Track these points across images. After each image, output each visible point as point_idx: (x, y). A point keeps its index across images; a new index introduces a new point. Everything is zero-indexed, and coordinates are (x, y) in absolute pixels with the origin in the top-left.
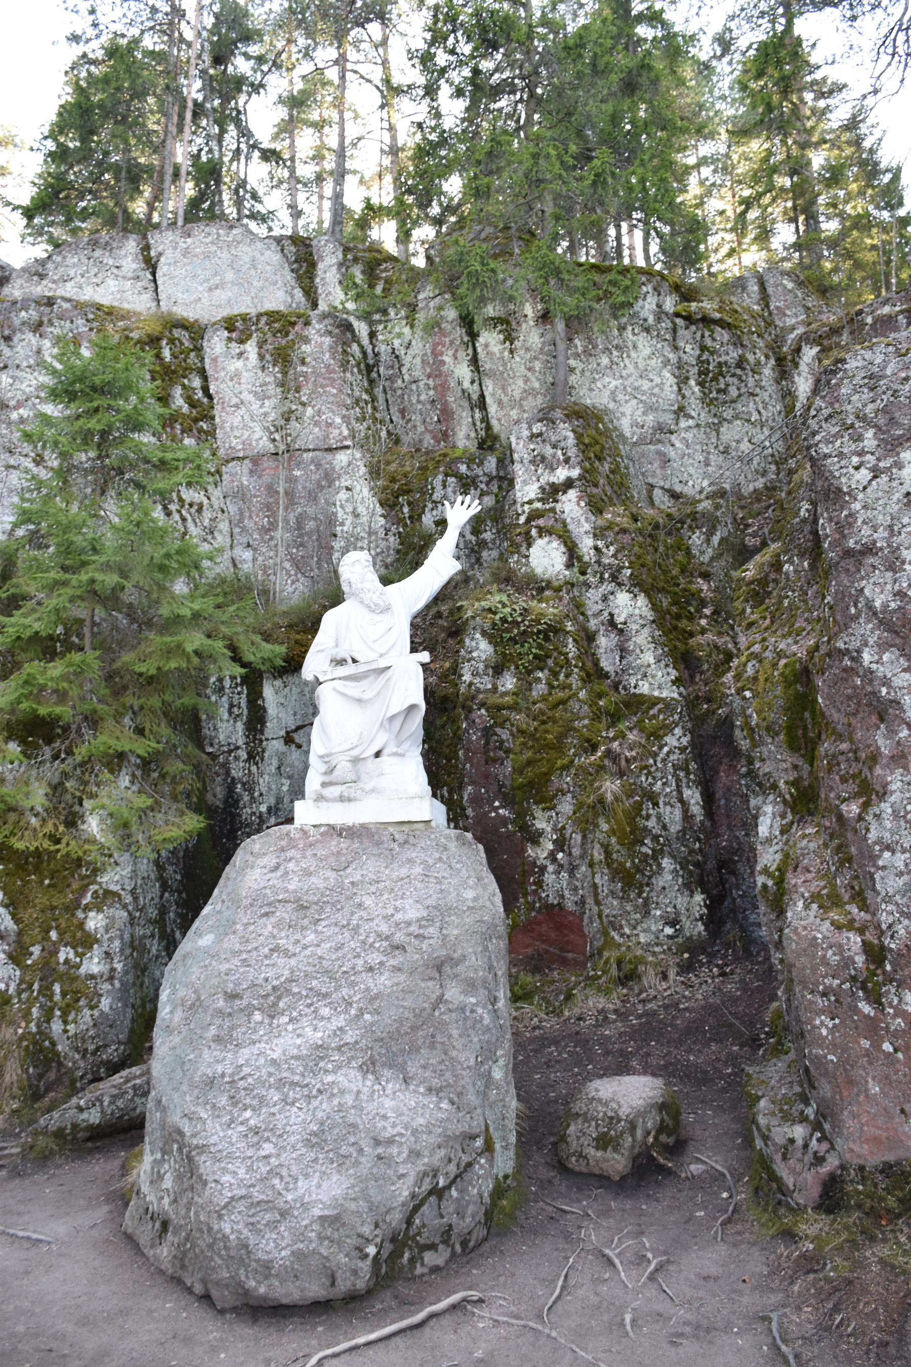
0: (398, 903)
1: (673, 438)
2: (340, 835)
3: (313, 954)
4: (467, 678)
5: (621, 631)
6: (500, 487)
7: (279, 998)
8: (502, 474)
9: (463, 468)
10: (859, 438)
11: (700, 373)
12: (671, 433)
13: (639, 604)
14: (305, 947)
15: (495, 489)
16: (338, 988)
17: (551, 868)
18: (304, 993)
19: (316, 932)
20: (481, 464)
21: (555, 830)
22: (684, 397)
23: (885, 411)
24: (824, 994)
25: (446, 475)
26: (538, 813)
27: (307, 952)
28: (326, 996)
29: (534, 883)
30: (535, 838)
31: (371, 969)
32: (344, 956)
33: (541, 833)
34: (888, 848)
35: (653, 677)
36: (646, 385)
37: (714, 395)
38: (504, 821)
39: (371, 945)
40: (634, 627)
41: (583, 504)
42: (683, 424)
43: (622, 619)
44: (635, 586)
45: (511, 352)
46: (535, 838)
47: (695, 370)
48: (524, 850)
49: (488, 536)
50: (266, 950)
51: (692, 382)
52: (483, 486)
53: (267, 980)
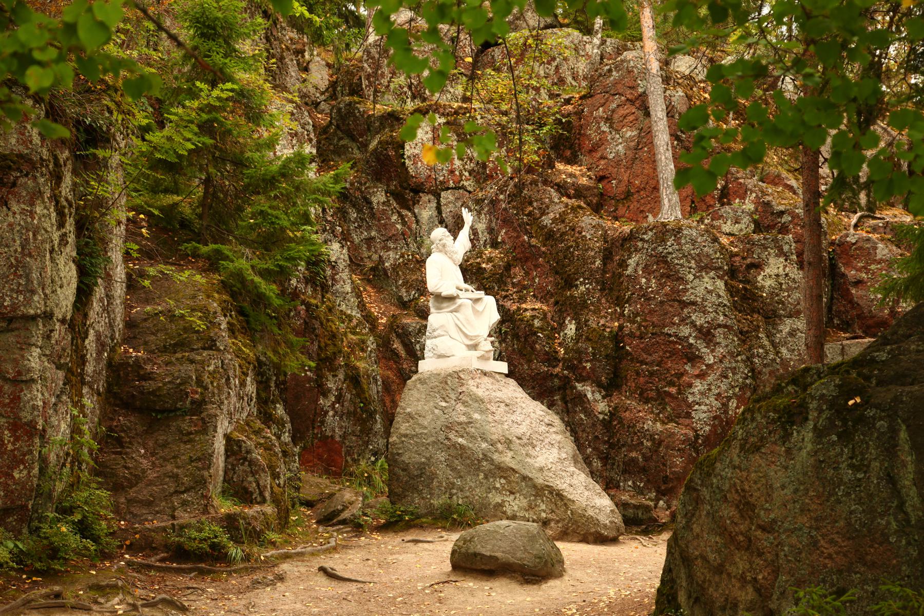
4: (294, 282)
5: (334, 267)
10: (689, 262)
13: (344, 251)
17: (331, 413)
21: (337, 389)
23: (698, 255)
24: (679, 450)
26: (330, 378)
29: (320, 422)
30: (325, 393)
33: (329, 390)
34: (697, 404)
38: (309, 379)
40: (342, 267)
43: (333, 259)
44: (343, 239)
46: (325, 393)
48: (318, 400)
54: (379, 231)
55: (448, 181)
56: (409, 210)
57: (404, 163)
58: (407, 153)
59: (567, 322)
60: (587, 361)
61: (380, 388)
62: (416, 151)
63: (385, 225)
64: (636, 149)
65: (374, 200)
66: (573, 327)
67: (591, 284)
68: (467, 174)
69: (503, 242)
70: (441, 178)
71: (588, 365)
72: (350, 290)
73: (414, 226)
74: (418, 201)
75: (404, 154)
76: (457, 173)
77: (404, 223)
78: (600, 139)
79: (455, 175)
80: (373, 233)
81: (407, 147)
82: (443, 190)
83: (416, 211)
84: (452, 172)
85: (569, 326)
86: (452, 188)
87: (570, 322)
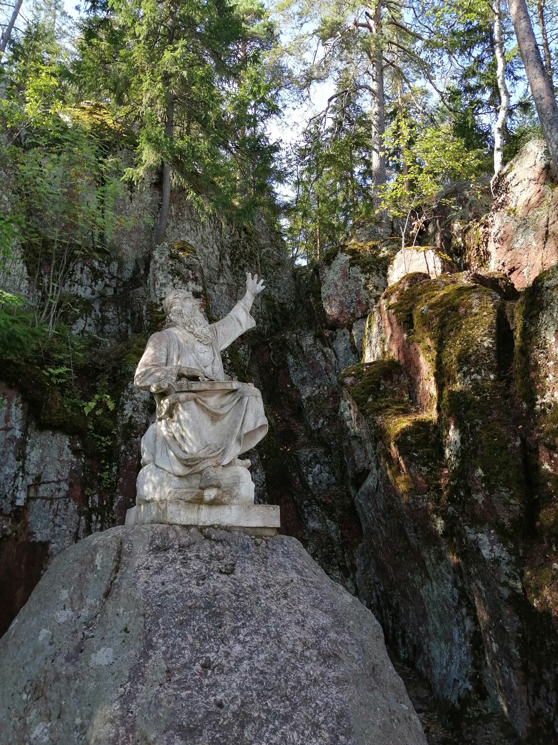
0: (301, 607)
1: (216, 287)
3: (253, 669)
6: (117, 284)
7: (242, 726)
8: (120, 276)
9: (96, 264)
11: (231, 254)
12: (215, 284)
14: (240, 661)
15: (114, 285)
16: (295, 707)
18: (263, 716)
19: (240, 642)
20: (108, 265)
22: (222, 265)
25: (85, 265)
27: (245, 665)
28: (286, 718)
31: (315, 682)
32: (283, 669)
36: (206, 251)
37: (237, 269)
39: (302, 654)
41: (203, 310)
42: (221, 281)
45: (131, 198)
47: (229, 251)
49: (110, 315)
50: (198, 667)
51: (228, 258)
52: (107, 280)
53: (220, 705)
54: (308, 371)
56: (330, 347)
58: (323, 295)
62: (330, 292)
63: (313, 363)
64: (547, 226)
65: (304, 344)
67: (479, 372)
70: (352, 311)
71: (480, 497)
73: (334, 359)
74: (336, 337)
76: (364, 303)
77: (326, 360)
80: (305, 374)
81: (323, 290)
82: (354, 321)
83: (334, 346)
84: (359, 302)
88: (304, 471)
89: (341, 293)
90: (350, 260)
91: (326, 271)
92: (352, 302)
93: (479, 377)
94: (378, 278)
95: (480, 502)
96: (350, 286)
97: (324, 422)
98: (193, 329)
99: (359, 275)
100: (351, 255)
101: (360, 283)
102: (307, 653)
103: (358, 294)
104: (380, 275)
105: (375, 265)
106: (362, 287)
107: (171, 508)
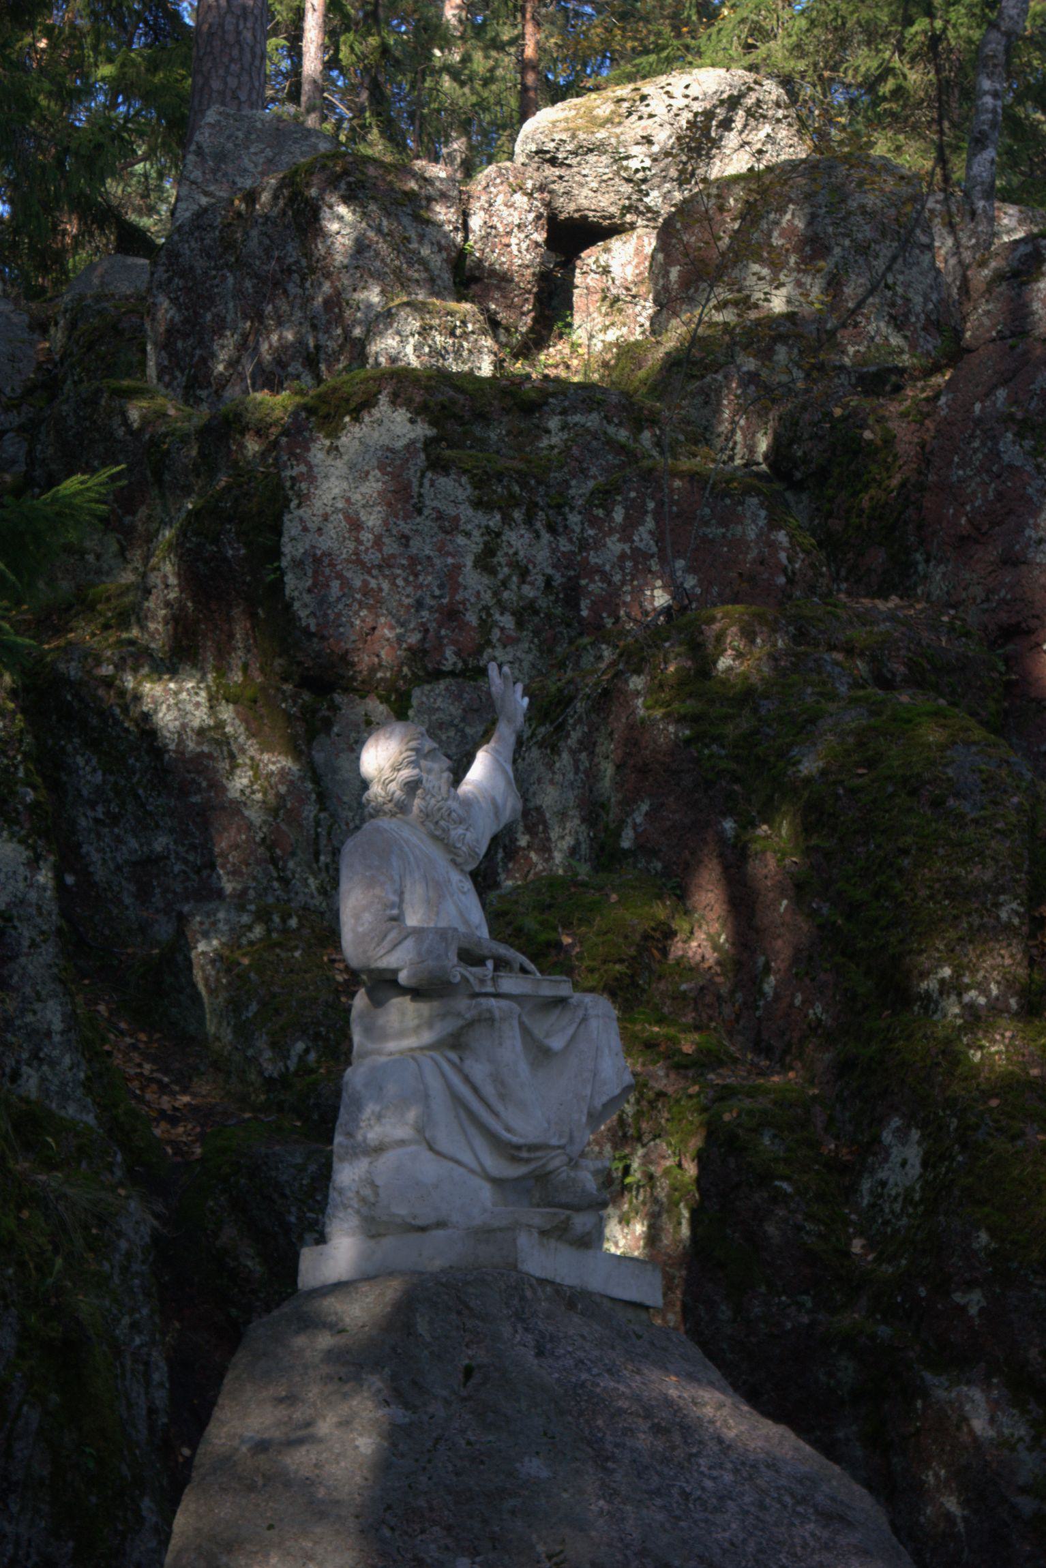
2: (571, 1305)
35: (53, 1063)
40: (27, 933)
55: (440, 647)
57: (279, 585)
58: (290, 550)
59: (887, 1137)
60: (970, 1285)
61: (161, 1397)
66: (914, 1154)
68: (507, 621)
69: (643, 848)
71: (974, 1301)
72: (58, 1025)
74: (328, 724)
75: (277, 554)
76: (472, 618)
78: (1000, 496)
79: (463, 626)
80: (161, 843)
81: (291, 527)
84: (452, 615)
85: (896, 1154)
86: (452, 674)
87: (902, 1136)
88: (293, 1219)
89: (373, 557)
90: (429, 443)
91: (317, 454)
92: (419, 604)
93: (982, 1000)
94: (528, 535)
95: (973, 1311)
96: (415, 543)
97: (307, 1051)
98: (446, 831)
99: (466, 512)
100: (433, 423)
101: (461, 540)
102: (800, 1509)
103: (451, 578)
104: (538, 525)
105: (524, 485)
106: (469, 561)
107: (524, 1241)
